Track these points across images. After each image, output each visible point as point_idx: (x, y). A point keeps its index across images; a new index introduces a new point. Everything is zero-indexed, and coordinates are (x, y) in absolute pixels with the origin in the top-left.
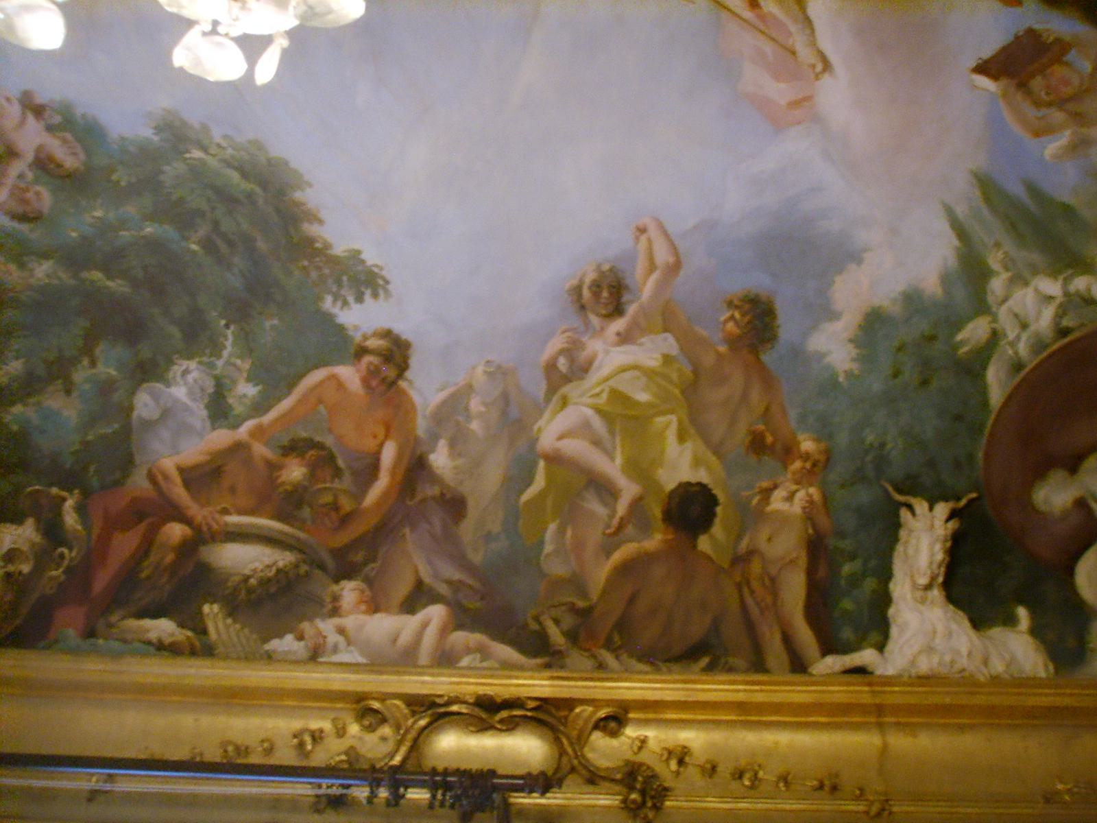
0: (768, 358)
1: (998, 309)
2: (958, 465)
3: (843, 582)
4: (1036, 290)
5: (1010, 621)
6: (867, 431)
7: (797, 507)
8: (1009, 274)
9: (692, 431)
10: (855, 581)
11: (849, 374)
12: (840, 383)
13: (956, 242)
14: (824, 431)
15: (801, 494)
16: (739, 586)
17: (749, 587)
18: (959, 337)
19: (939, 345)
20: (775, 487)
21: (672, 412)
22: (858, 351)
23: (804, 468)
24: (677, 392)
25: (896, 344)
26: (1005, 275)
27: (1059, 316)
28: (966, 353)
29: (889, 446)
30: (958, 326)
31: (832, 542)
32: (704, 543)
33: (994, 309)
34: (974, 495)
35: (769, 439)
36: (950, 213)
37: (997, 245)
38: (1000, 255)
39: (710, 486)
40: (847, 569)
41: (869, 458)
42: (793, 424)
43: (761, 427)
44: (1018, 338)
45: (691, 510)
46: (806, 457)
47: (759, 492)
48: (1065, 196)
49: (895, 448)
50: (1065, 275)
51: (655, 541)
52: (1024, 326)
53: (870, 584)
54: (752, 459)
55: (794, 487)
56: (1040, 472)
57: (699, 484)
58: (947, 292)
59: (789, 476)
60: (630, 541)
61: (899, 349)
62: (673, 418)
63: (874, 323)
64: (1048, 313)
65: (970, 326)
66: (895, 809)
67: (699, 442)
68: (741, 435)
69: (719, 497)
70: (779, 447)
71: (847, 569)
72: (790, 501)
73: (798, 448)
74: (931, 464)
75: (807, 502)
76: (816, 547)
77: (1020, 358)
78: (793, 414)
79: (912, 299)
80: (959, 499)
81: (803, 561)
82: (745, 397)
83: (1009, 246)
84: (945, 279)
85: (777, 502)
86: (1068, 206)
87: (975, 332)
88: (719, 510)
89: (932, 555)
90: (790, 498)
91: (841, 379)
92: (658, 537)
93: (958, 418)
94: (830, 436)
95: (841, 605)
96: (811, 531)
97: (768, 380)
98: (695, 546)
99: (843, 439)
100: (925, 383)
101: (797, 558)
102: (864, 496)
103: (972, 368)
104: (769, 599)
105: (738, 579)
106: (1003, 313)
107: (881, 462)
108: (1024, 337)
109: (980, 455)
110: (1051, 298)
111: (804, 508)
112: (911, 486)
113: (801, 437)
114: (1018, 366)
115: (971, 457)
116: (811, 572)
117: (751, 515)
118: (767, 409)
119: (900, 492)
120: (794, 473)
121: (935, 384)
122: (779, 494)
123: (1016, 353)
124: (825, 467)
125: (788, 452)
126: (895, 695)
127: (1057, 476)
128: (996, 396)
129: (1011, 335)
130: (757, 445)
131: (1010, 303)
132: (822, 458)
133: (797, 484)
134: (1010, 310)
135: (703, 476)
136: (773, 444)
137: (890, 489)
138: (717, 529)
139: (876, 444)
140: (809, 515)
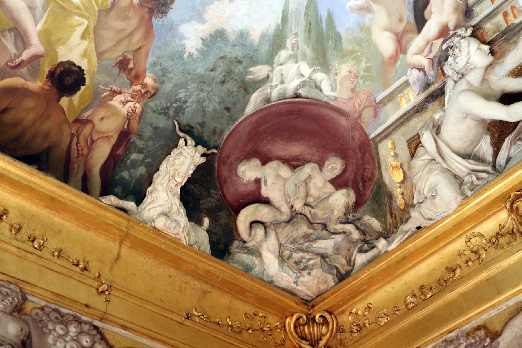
0: (156, 21)
1: (277, 66)
2: (214, 132)
3: (128, 163)
4: (299, 67)
5: (199, 223)
6: (182, 90)
7: (125, 110)
8: (293, 53)
9: (92, 36)
10: (135, 164)
11: (190, 56)
12: (184, 58)
13: (280, 22)
14: (160, 80)
15: (131, 104)
16: (72, 135)
17: (78, 139)
18: (252, 69)
19: (240, 68)
20: (120, 93)
21: (87, 19)
22: (202, 46)
23: (140, 91)
24: (97, 9)
25: (222, 55)
26: (290, 52)
27: (300, 86)
28: (250, 79)
29: (188, 104)
30: (254, 63)
31: (133, 138)
32: (64, 101)
33: (275, 66)
34: (215, 151)
35: (131, 65)
36: (287, 4)
37: (296, 35)
38: (294, 41)
39: (85, 72)
40: (134, 156)
41: (175, 105)
42: (148, 65)
43: (130, 56)
44: (276, 85)
45: (67, 79)
46: (145, 86)
47: (110, 91)
48: (341, 30)
49: (191, 107)
50: (316, 68)
51: (37, 85)
52: (282, 82)
53: (142, 170)
54: (116, 70)
55: (130, 98)
56: (248, 156)
57: (79, 67)
58: (260, 44)
59: (130, 91)
60: (21, 77)
61: (221, 58)
62: (86, 22)
63: (219, 35)
64: (297, 82)
65: (259, 67)
66: (112, 292)
67: (93, 44)
68: (117, 54)
69: (87, 81)
70: (133, 73)
71: (134, 156)
72: (123, 105)
73: (143, 79)
74: (202, 125)
75: (132, 110)
76: (124, 136)
77: (271, 96)
78: (151, 59)
79: (243, 35)
80: (208, 149)
81: (113, 141)
82: (130, 35)
83: (301, 38)
84: (263, 36)
85: (116, 101)
86: (340, 35)
87: (260, 71)
88: (83, 88)
89: (188, 170)
90: (125, 103)
91: (185, 56)
92: (39, 84)
93: (228, 109)
94: (163, 82)
95: (122, 174)
96: (126, 126)
97: (149, 32)
98: (59, 101)
99: (168, 87)
100: (223, 82)
101: (112, 136)
102: (162, 122)
103: (247, 88)
104: (85, 151)
105: (74, 131)
106: (278, 69)
107: (179, 110)
108: (279, 87)
109: (227, 133)
110: (302, 75)
111: (128, 112)
112: (188, 130)
113: (148, 74)
114: (268, 100)
115: (222, 132)
116: (115, 147)
117: (99, 100)
118: (139, 48)
119: (181, 130)
120: (133, 91)
121: (227, 86)
122: (119, 98)
123: (271, 93)
124: (151, 97)
125: (137, 78)
126: (137, 232)
127: (256, 162)
128: (250, 109)
129: (274, 83)
130: (123, 64)
131: (284, 66)
132: (152, 92)
133: (132, 98)
134: (281, 70)
135: (84, 64)
136: (131, 69)
137: (177, 126)
138: (76, 98)
139: (183, 99)
140: (128, 119)
